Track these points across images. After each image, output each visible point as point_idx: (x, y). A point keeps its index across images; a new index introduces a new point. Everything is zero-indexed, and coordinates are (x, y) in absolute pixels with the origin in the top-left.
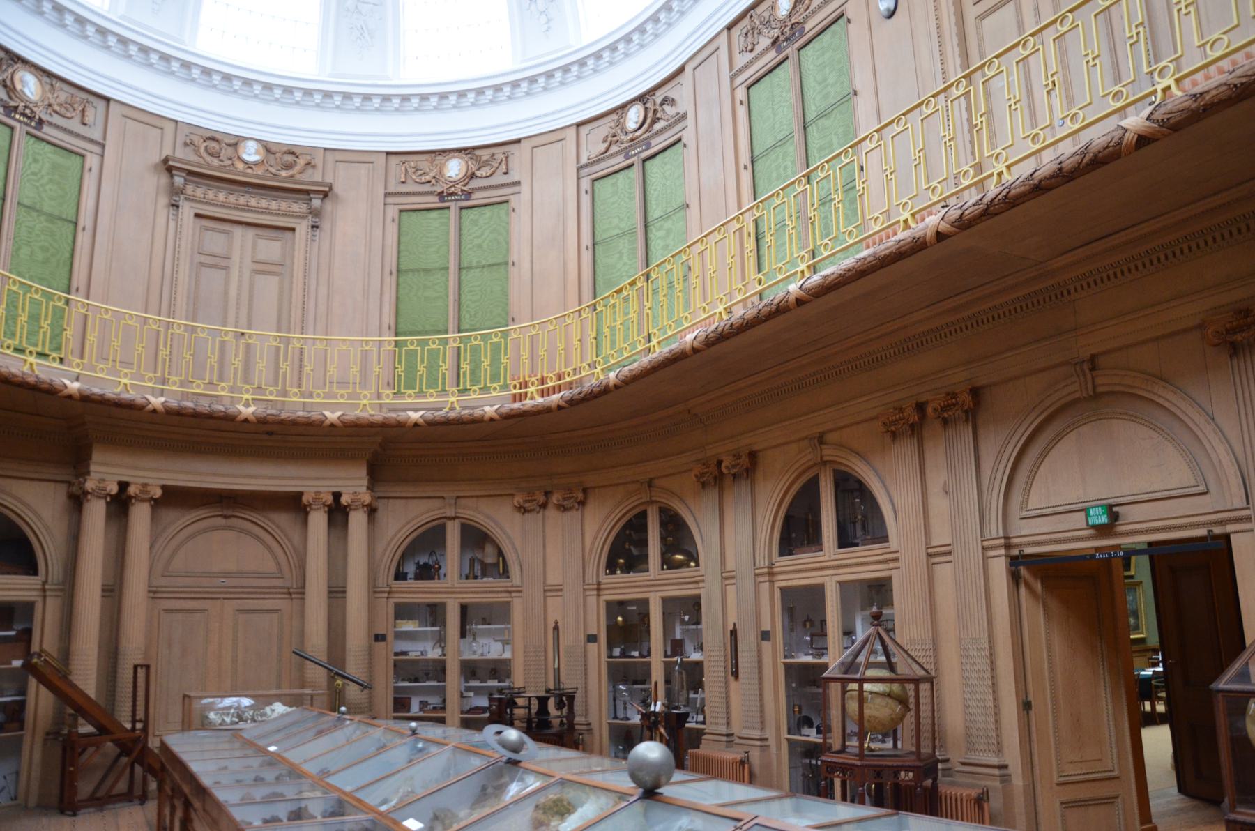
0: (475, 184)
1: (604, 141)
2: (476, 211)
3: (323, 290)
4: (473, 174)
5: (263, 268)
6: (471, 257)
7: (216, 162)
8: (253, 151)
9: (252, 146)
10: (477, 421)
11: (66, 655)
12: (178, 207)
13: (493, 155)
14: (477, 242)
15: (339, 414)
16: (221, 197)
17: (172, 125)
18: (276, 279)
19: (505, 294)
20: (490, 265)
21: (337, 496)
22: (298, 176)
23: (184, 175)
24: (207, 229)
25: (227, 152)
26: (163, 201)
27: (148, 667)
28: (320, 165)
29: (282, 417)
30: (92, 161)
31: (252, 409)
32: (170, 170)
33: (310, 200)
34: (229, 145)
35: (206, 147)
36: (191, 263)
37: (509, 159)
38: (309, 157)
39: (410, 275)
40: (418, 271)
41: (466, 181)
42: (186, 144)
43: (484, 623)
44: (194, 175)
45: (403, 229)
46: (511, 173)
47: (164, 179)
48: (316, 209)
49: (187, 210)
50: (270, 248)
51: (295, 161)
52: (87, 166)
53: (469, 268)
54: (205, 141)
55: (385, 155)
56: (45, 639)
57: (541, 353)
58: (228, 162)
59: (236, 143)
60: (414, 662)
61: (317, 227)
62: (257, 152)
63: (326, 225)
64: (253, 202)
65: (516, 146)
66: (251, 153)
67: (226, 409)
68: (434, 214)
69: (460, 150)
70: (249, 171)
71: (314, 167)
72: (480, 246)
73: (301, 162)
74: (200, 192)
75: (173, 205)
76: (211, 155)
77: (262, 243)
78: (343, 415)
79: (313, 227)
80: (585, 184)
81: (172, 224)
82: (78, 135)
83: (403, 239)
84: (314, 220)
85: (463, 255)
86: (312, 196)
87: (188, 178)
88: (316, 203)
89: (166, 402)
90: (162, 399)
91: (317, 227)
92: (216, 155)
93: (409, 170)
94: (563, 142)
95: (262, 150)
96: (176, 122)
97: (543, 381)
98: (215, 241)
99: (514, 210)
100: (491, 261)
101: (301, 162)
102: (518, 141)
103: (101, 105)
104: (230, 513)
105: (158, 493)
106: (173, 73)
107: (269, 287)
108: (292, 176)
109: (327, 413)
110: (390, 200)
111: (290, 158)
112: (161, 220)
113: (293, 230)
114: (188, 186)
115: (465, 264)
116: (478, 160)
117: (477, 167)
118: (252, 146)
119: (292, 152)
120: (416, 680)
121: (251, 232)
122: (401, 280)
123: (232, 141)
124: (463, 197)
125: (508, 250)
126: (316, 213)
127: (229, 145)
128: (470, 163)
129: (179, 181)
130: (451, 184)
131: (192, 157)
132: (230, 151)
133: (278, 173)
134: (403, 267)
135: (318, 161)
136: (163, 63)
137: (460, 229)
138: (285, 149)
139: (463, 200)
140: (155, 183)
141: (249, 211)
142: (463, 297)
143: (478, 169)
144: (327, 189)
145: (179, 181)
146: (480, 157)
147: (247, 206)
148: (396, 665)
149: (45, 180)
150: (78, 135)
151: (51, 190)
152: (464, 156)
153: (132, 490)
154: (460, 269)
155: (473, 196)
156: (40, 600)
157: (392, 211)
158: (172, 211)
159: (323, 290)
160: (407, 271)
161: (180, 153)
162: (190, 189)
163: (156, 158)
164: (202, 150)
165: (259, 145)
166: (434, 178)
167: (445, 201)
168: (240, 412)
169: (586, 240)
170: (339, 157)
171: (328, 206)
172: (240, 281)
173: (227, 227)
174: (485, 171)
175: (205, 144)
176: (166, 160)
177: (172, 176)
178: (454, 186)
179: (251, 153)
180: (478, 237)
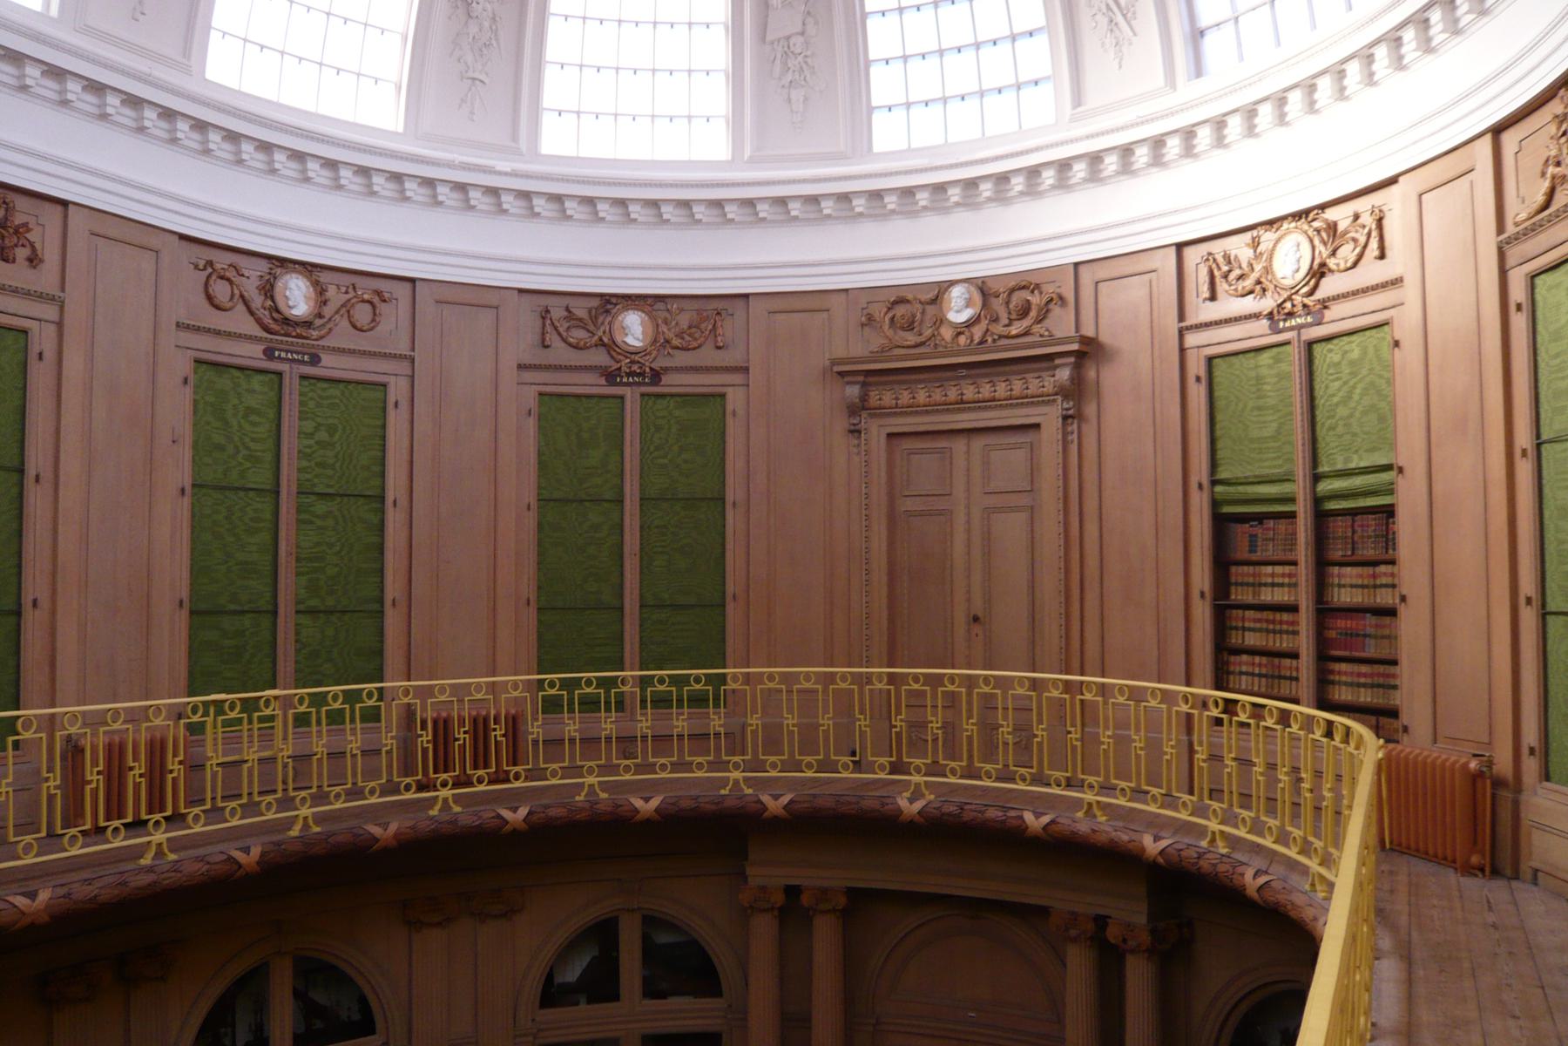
0: (1329, 287)
1: (1543, 174)
3: (1092, 529)
4: (1323, 265)
7: (911, 338)
8: (961, 303)
9: (957, 292)
12: (859, 432)
13: (1356, 217)
15: (1046, 819)
21: (1101, 921)
23: (861, 378)
24: (911, 453)
28: (1070, 297)
29: (965, 819)
30: (735, 399)
31: (918, 806)
33: (1056, 367)
35: (892, 319)
37: (1386, 222)
41: (1312, 282)
44: (872, 377)
46: (1388, 253)
49: (876, 431)
51: (1028, 301)
54: (889, 309)
55: (1174, 248)
58: (928, 333)
63: (1090, 410)
65: (1394, 189)
67: (883, 805)
69: (1297, 216)
74: (888, 398)
75: (851, 432)
76: (903, 329)
78: (1053, 822)
79: (1065, 418)
84: (1065, 406)
86: (1057, 361)
87: (871, 379)
89: (791, 802)
90: (785, 800)
92: (910, 326)
93: (1217, 273)
99: (1397, 344)
102: (1392, 181)
105: (842, 901)
108: (1027, 333)
109: (1029, 817)
113: (1037, 426)
114: (872, 394)
116: (1332, 227)
117: (1330, 249)
119: (1025, 283)
123: (931, 295)
124: (1309, 319)
126: (1076, 391)
128: (1317, 241)
130: (1285, 295)
131: (876, 342)
132: (931, 310)
138: (1012, 284)
141: (964, 410)
143: (1334, 253)
144: (1075, 347)
146: (1335, 224)
147: (962, 402)
149: (676, 448)
151: (686, 461)
152: (1306, 227)
153: (806, 899)
155: (1329, 315)
165: (972, 289)
166: (1259, 282)
167: (1280, 331)
173: (942, 443)
174: (1347, 253)
175: (890, 315)
178: (1289, 298)
179: (959, 310)
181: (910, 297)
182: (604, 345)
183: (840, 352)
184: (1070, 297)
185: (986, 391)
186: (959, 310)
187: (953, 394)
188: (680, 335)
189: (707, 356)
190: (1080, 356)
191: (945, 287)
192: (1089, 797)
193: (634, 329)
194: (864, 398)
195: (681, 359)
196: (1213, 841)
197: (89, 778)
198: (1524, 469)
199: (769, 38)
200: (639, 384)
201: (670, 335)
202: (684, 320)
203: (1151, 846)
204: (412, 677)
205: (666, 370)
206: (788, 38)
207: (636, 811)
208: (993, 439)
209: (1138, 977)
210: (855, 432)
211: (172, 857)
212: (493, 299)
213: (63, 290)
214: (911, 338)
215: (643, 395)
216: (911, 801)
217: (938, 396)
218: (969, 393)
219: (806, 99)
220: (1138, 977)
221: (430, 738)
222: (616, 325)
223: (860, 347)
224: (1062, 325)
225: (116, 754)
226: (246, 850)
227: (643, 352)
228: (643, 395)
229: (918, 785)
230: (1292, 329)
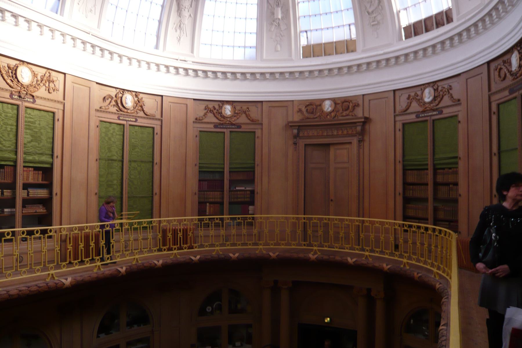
7: (311, 116)
12: (296, 144)
15: (354, 260)
17: (292, 102)
21: (369, 290)
30: (258, 133)
33: (357, 126)
42: (298, 112)
44: (300, 128)
49: (302, 143)
52: (256, 136)
61: (361, 141)
62: (331, 106)
63: (366, 138)
66: (327, 107)
71: (358, 105)
75: (294, 143)
78: (356, 261)
79: (359, 141)
80: (494, 108)
86: (358, 124)
91: (361, 141)
92: (312, 113)
94: (482, 75)
96: (293, 101)
109: (349, 259)
110: (398, 118)
113: (351, 143)
123: (318, 103)
126: (363, 132)
135: (361, 103)
144: (363, 120)
157: (399, 126)
164: (305, 113)
168: (310, 258)
169: (495, 149)
175: (306, 108)
183: (290, 119)
186: (327, 107)
191: (323, 100)
192: (367, 253)
194: (298, 133)
196: (405, 265)
197: (91, 244)
198: (495, 159)
203: (386, 267)
204: (161, 217)
207: (231, 257)
209: (380, 307)
210: (295, 144)
211: (102, 269)
213: (64, 99)
215: (230, 132)
216: (313, 255)
220: (380, 307)
221: (182, 234)
223: (297, 118)
224: (359, 112)
225: (76, 239)
226: (122, 268)
228: (230, 132)
229: (315, 250)
230: (427, 116)
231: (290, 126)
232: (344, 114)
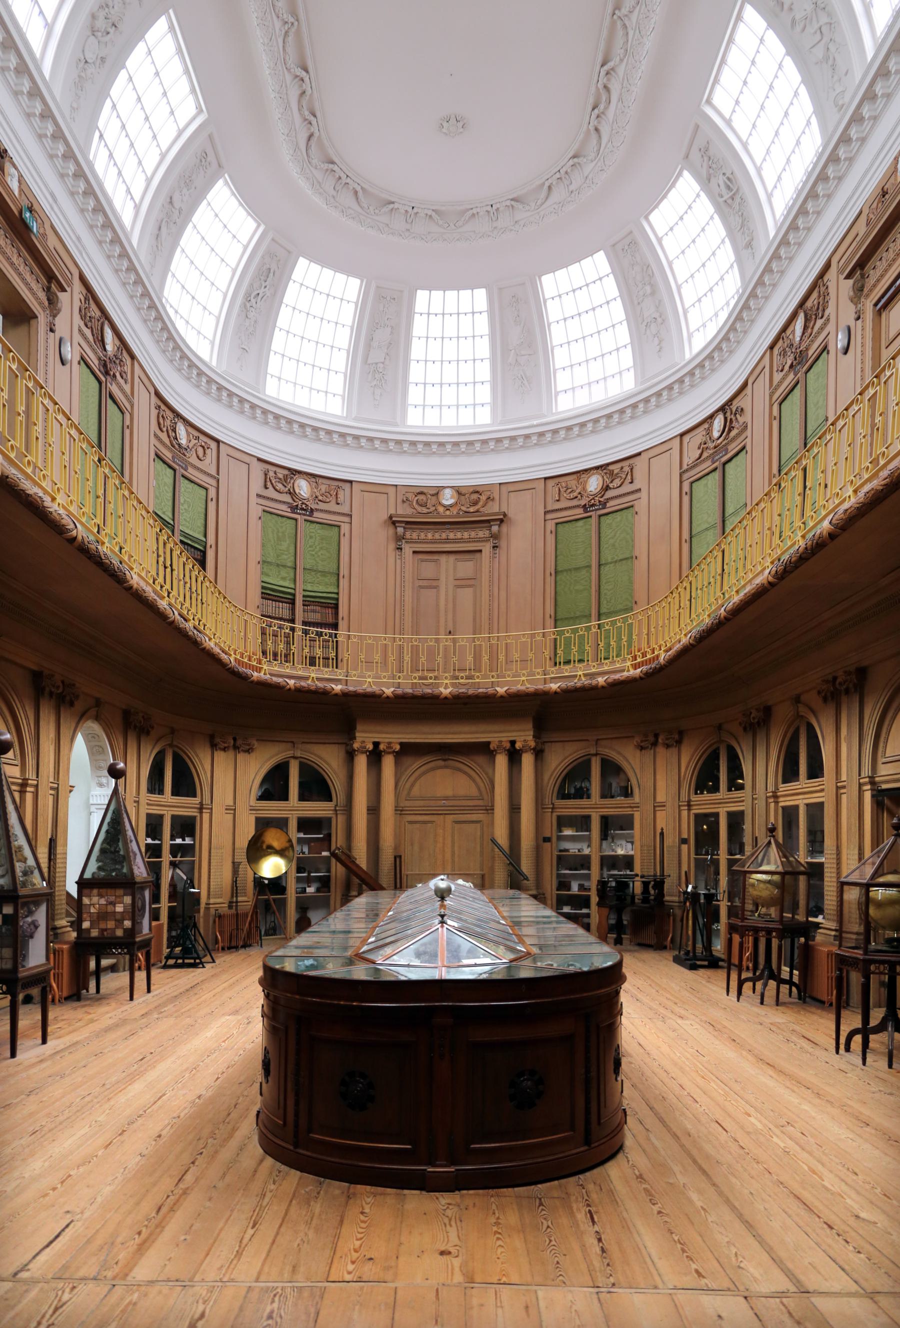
2: (610, 517)
3: (503, 594)
5: (463, 583)
6: (607, 556)
7: (425, 510)
8: (449, 496)
9: (448, 493)
10: (594, 688)
11: (349, 848)
14: (611, 541)
16: (430, 536)
17: (394, 488)
18: (471, 590)
19: (631, 582)
20: (621, 560)
22: (481, 510)
25: (432, 501)
26: (392, 546)
27: (400, 857)
28: (497, 498)
30: (345, 528)
32: (394, 523)
33: (491, 526)
34: (433, 495)
36: (413, 588)
38: (489, 493)
39: (565, 574)
40: (570, 570)
43: (622, 829)
45: (559, 538)
47: (391, 530)
48: (495, 534)
49: (408, 549)
50: (465, 567)
53: (606, 564)
56: (338, 840)
57: (653, 630)
59: (437, 491)
60: (575, 856)
63: (503, 543)
64: (451, 536)
66: (448, 498)
68: (580, 523)
70: (448, 513)
71: (493, 499)
72: (614, 545)
73: (483, 498)
74: (415, 535)
76: (421, 505)
77: (459, 564)
79: (494, 547)
81: (398, 561)
82: (334, 513)
83: (559, 547)
85: (602, 554)
88: (495, 529)
92: (424, 505)
95: (455, 494)
97: (635, 658)
98: (428, 569)
100: (621, 557)
101: (483, 498)
103: (348, 485)
104: (447, 757)
106: (391, 450)
107: (466, 595)
108: (477, 511)
111: (475, 496)
112: (391, 560)
113: (480, 551)
115: (603, 562)
118: (448, 493)
119: (476, 491)
120: (576, 870)
121: (452, 558)
122: (558, 578)
125: (633, 546)
126: (495, 537)
127: (433, 495)
129: (400, 530)
131: (409, 511)
132: (434, 498)
133: (467, 510)
134: (559, 569)
136: (384, 445)
137: (599, 533)
139: (600, 509)
140: (385, 534)
142: (602, 587)
145: (400, 530)
148: (559, 858)
150: (334, 513)
154: (600, 565)
156: (334, 816)
158: (398, 553)
159: (503, 594)
160: (562, 571)
161: (400, 512)
162: (408, 535)
163: (386, 517)
164: (415, 504)
169: (686, 535)
170: (511, 488)
171: (504, 528)
172: (446, 595)
173: (436, 557)
176: (391, 517)
177: (396, 527)
180: (612, 538)
181: (425, 490)
182: (290, 493)
184: (497, 498)
185: (459, 535)
186: (448, 498)
187: (444, 536)
188: (322, 495)
189: (332, 507)
190: (502, 521)
193: (303, 488)
195: (322, 506)
198: (686, 547)
199: (369, 362)
200: (304, 515)
201: (318, 494)
202: (323, 488)
205: (317, 510)
206: (377, 364)
208: (458, 556)
212: (247, 459)
214: (425, 510)
217: (437, 536)
218: (451, 536)
219: (381, 395)
222: (296, 485)
223: (404, 511)
227: (308, 500)
231: (393, 522)
232: (472, 510)
